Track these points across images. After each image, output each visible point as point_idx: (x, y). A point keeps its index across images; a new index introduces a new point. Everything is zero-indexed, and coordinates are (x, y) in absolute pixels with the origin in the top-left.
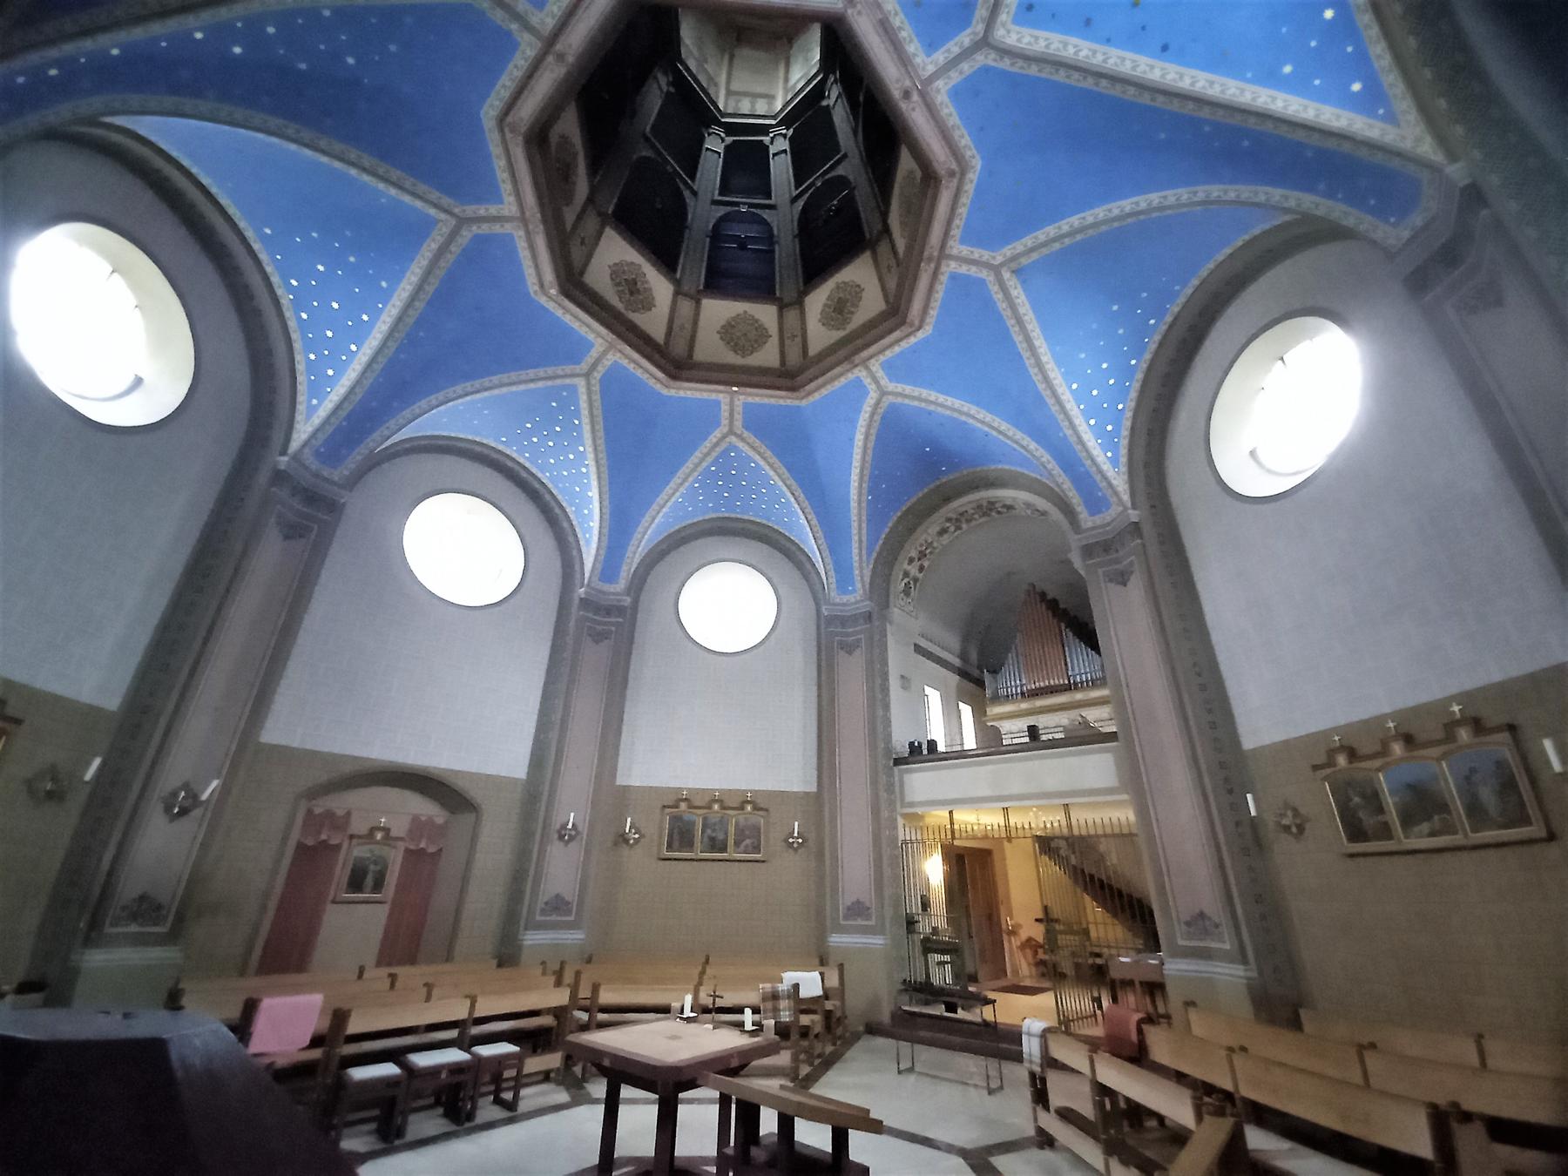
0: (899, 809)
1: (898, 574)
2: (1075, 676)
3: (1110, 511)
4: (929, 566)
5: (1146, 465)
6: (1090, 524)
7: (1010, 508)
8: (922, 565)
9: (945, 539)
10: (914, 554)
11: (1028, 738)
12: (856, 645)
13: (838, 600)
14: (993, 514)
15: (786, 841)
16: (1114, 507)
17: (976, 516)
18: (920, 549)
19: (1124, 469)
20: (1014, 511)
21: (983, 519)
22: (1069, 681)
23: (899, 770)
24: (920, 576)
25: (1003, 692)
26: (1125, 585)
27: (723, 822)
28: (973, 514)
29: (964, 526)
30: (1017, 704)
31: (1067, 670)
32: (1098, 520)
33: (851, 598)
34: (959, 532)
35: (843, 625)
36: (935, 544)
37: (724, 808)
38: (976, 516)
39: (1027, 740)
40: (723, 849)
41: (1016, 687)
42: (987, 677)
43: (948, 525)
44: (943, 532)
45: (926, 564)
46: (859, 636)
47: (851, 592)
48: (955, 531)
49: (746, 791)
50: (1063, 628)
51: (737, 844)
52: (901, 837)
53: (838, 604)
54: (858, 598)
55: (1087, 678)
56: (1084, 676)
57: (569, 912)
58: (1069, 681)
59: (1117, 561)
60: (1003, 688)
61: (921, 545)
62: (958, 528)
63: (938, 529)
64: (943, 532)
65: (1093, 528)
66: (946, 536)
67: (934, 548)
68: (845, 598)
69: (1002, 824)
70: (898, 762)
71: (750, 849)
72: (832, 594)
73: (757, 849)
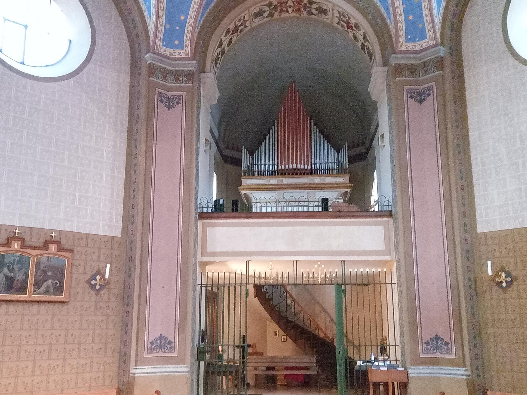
4: (235, 42)
5: (454, 14)
6: (404, 48)
8: (231, 39)
10: (232, 27)
12: (178, 100)
13: (162, 51)
14: (305, 13)
15: (89, 282)
16: (428, 39)
18: (237, 23)
19: (441, 11)
20: (324, 16)
21: (294, 14)
22: (312, 167)
24: (226, 49)
25: (256, 168)
27: (23, 262)
28: (290, 7)
29: (276, 15)
31: (311, 158)
32: (411, 46)
33: (177, 53)
34: (269, 18)
36: (248, 24)
37: (23, 246)
38: (290, 10)
39: (320, 209)
40: (23, 289)
41: (269, 165)
43: (267, 9)
44: (259, 14)
45: (234, 40)
47: (176, 47)
49: (52, 231)
51: (38, 284)
54: (183, 55)
55: (325, 166)
58: (312, 167)
59: (417, 83)
61: (239, 21)
63: (257, 10)
66: (258, 19)
67: (246, 27)
68: (169, 51)
69: (244, 273)
70: (202, 216)
71: (52, 290)
72: (158, 43)
73: (59, 290)
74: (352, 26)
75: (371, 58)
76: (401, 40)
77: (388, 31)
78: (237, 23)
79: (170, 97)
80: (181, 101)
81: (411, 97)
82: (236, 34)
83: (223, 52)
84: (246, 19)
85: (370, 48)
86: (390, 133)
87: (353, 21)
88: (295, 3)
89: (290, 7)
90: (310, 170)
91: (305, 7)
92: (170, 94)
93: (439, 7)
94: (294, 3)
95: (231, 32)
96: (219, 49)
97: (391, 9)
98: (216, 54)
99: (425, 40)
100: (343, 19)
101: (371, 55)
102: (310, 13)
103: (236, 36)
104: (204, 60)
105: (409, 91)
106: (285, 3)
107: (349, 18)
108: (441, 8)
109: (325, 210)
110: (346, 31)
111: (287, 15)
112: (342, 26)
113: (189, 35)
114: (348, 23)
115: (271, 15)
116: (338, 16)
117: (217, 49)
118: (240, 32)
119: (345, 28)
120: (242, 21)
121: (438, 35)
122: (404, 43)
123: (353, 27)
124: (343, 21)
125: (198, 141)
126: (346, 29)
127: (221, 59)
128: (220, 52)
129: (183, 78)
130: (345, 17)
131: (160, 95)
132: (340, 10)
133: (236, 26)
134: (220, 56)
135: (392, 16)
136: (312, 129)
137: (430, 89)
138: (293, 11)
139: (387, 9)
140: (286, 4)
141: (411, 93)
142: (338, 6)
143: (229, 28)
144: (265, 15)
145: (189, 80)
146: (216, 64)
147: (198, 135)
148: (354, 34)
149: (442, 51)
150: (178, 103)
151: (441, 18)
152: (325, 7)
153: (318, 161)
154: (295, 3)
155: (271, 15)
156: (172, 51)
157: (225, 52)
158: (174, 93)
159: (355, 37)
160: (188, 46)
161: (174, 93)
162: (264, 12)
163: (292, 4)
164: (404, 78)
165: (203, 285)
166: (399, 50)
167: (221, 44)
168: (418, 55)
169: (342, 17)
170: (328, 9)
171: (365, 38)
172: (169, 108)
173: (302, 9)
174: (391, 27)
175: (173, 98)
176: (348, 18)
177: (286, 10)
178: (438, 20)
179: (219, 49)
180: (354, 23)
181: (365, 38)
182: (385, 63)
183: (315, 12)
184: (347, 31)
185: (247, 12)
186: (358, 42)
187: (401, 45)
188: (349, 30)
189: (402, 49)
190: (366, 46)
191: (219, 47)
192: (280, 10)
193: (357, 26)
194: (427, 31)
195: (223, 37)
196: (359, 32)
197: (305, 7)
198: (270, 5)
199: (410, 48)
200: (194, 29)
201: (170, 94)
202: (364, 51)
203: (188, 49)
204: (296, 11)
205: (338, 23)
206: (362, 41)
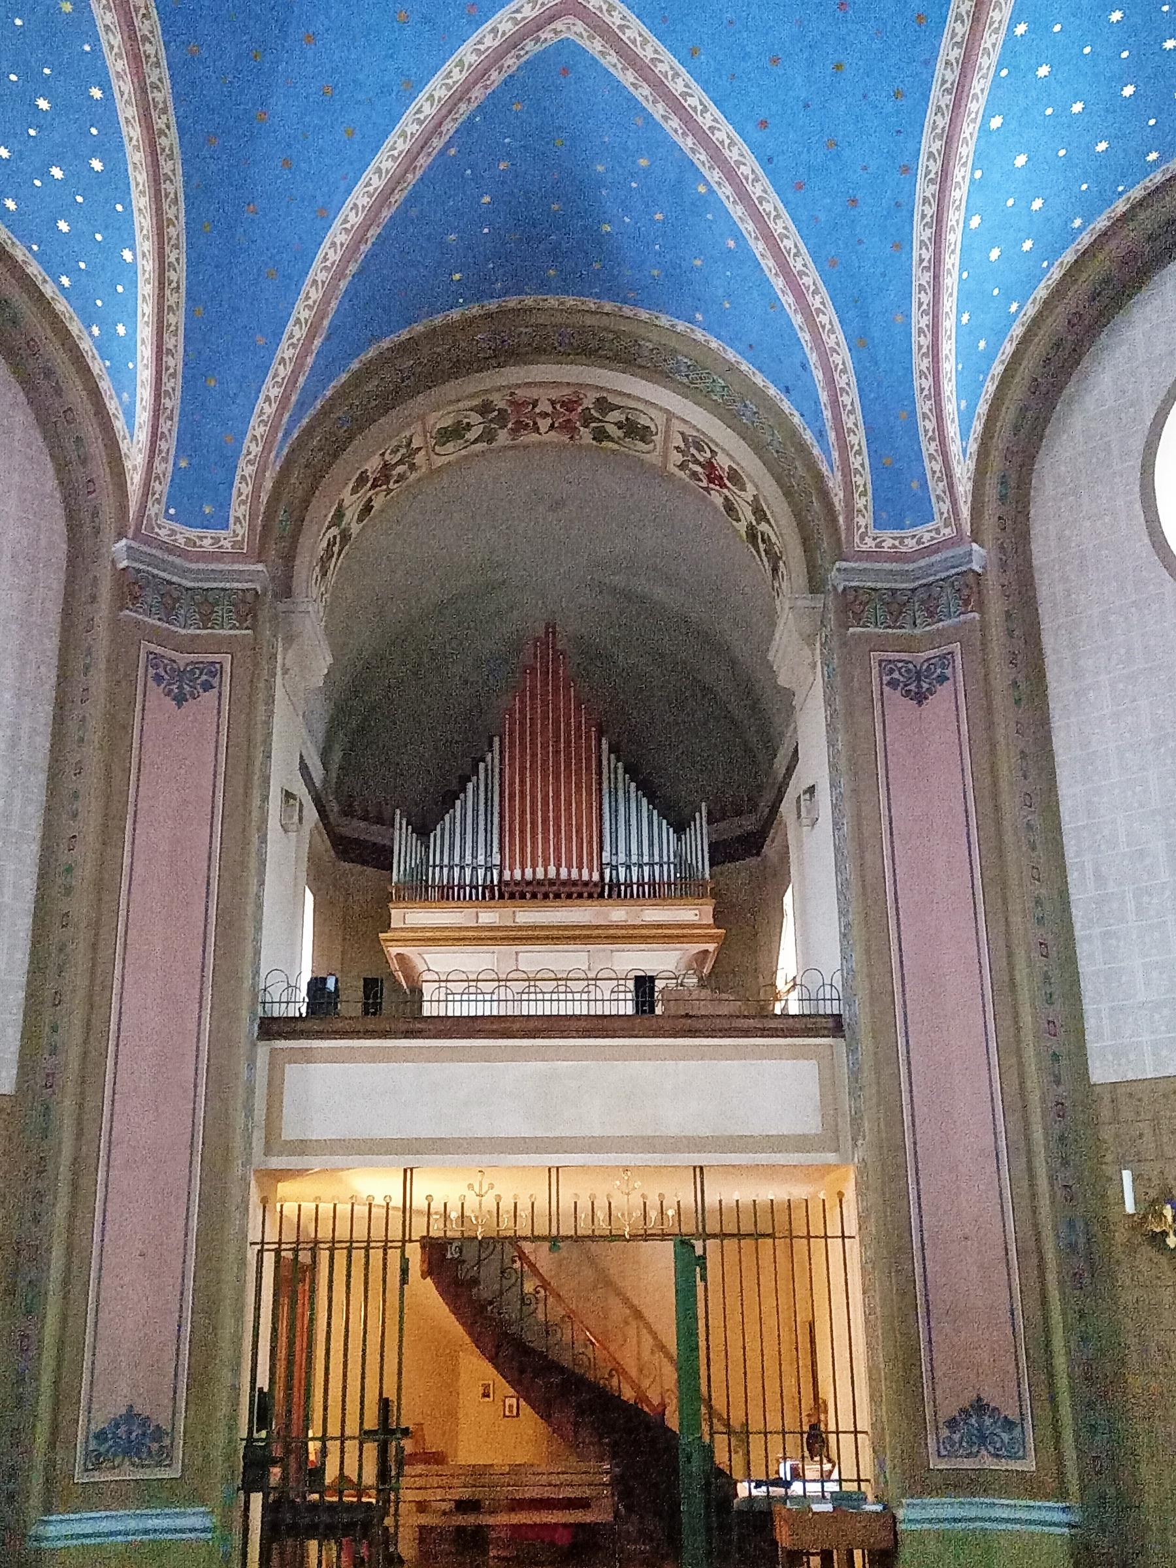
1: (321, 510)
3: (919, 530)
5: (1009, 454)
6: (869, 544)
7: (634, 430)
8: (370, 500)
9: (451, 451)
10: (373, 465)
16: (938, 522)
17: (544, 424)
19: (973, 447)
20: (641, 446)
24: (355, 528)
25: (437, 876)
26: (920, 703)
28: (545, 415)
29: (503, 437)
31: (601, 849)
35: (169, 611)
36: (419, 459)
38: (544, 424)
39: (629, 1009)
41: (474, 869)
42: (403, 842)
43: (475, 418)
44: (455, 432)
45: (377, 504)
46: (143, 655)
48: (475, 441)
50: (605, 746)
53: (171, 549)
57: (163, 1457)
60: (434, 866)
61: (395, 451)
63: (448, 422)
64: (455, 432)
65: (869, 556)
66: (450, 447)
67: (413, 467)
68: (183, 534)
69: (397, 1202)
74: (721, 478)
75: (775, 570)
77: (824, 495)
78: (387, 457)
80: (215, 682)
81: (893, 684)
82: (384, 487)
83: (345, 536)
84: (414, 446)
85: (774, 539)
87: (722, 461)
88: (558, 406)
89: (545, 415)
90: (596, 885)
92: (183, 659)
93: (964, 435)
95: (369, 485)
96: (334, 531)
97: (832, 436)
98: (324, 544)
99: (930, 526)
101: (775, 559)
102: (601, 435)
104: (289, 558)
108: (971, 439)
109: (644, 1012)
111: (535, 437)
112: (694, 475)
113: (247, 490)
114: (710, 466)
115: (488, 436)
116: (682, 446)
117: (329, 528)
119: (700, 480)
120: (403, 451)
121: (965, 512)
124: (697, 462)
125: (265, 798)
126: (704, 484)
127: (339, 555)
128: (335, 537)
130: (700, 450)
131: (155, 660)
133: (385, 465)
134: (336, 549)
135: (835, 454)
136: (605, 762)
137: (946, 659)
138: (552, 426)
139: (821, 435)
140: (534, 407)
141: (891, 671)
144: (471, 435)
145: (242, 619)
147: (266, 780)
148: (726, 498)
149: (979, 556)
150: (207, 686)
151: (972, 466)
152: (643, 421)
153: (622, 858)
154: (558, 406)
155: (488, 436)
156: (193, 533)
159: (730, 508)
163: (549, 410)
164: (872, 629)
165: (266, 1247)
167: (339, 514)
168: (910, 567)
169: (693, 451)
170: (653, 429)
172: (180, 700)
174: (835, 483)
175: (192, 672)
176: (708, 455)
178: (963, 470)
179: (334, 531)
182: (815, 585)
184: (706, 489)
185: (417, 427)
188: (711, 486)
189: (864, 548)
193: (734, 477)
194: (933, 500)
195: (346, 494)
196: (742, 494)
197: (587, 420)
201: (183, 659)
203: (242, 530)
204: (561, 427)
205: (682, 466)
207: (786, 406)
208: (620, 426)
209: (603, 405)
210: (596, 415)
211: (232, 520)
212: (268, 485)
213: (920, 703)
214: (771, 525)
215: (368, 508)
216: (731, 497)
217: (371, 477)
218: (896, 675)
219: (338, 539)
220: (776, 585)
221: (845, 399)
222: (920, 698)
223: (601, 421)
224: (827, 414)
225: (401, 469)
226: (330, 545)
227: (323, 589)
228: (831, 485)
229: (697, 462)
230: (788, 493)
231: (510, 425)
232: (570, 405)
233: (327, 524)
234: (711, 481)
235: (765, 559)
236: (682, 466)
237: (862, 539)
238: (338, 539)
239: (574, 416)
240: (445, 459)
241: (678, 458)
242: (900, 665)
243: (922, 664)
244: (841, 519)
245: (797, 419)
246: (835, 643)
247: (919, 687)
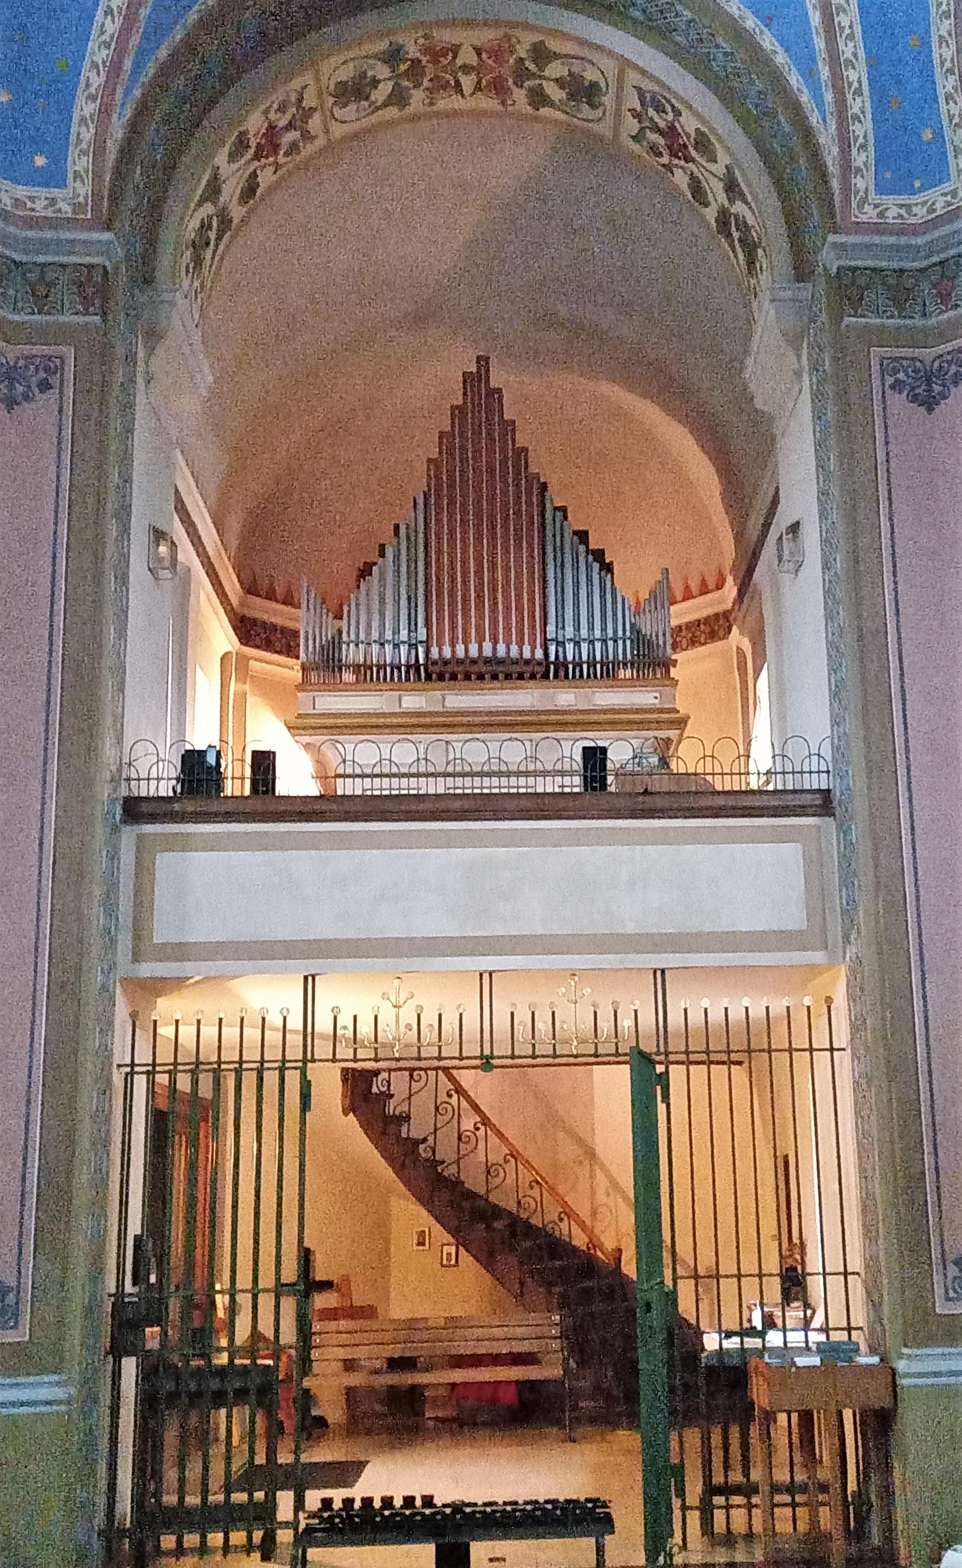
0: (124, 966)
2: (560, 644)
3: (931, 195)
4: (271, 189)
6: (869, 214)
8: (254, 175)
10: (255, 124)
11: (577, 780)
14: (520, 96)
18: (272, 116)
20: (586, 110)
23: (140, 837)
26: (930, 410)
28: (466, 69)
29: (418, 97)
30: (396, 694)
36: (315, 123)
38: (468, 82)
43: (382, 71)
52: (121, 1055)
56: (584, 646)
61: (282, 109)
62: (398, 98)
63: (346, 74)
74: (685, 146)
75: (751, 262)
76: (859, 183)
77: (815, 154)
78: (272, 116)
79: (12, 363)
81: (897, 386)
82: (271, 159)
83: (225, 222)
85: (750, 220)
86: (823, 515)
87: (689, 124)
88: (484, 56)
89: (466, 69)
91: (521, 74)
94: (479, 54)
95: (252, 151)
97: (825, 73)
98: (195, 224)
100: (657, 119)
101: (750, 248)
102: (538, 98)
103: (272, 169)
105: (890, 366)
106: (450, 57)
107: (677, 113)
110: (664, 165)
111: (456, 102)
112: (654, 150)
113: (88, 135)
114: (671, 132)
116: (639, 108)
117: (200, 204)
118: (287, 154)
119: (660, 154)
122: (872, 194)
123: (691, 149)
124: (657, 129)
125: (125, 531)
126: (665, 160)
127: (217, 246)
128: (210, 217)
129: (65, 293)
130: (660, 110)
132: (648, 86)
133: (271, 127)
134: (212, 235)
135: (829, 97)
138: (478, 88)
139: (810, 74)
141: (895, 371)
142: (637, 67)
143: (242, 134)
146: (198, 261)
147: (124, 512)
150: (45, 386)
152: (590, 75)
155: (398, 98)
157: (233, 225)
158: (27, 349)
160: (85, 177)
161: (27, 349)
162: (375, 83)
163: (473, 60)
166: (853, 219)
167: (213, 190)
168: (920, 241)
169: (651, 112)
170: (603, 85)
171: (732, 187)
173: (510, 81)
174: (827, 137)
176: (670, 116)
177: (452, 83)
179: (208, 208)
180: (693, 134)
181: (732, 187)
183: (555, 93)
184: (668, 168)
186: (706, 205)
187: (864, 201)
188: (676, 161)
189: (864, 218)
190: (736, 217)
191: (206, 200)
192: (431, 80)
193: (703, 143)
195: (221, 159)
196: (712, 167)
197: (521, 74)
198: (393, 56)
199: (890, 214)
200: (105, 111)
202: (729, 235)
205: (637, 138)
206: (722, 197)
207: (768, 41)
208: (560, 82)
209: (541, 54)
210: (532, 67)
211: (70, 175)
212: (117, 132)
213: (930, 410)
214: (747, 203)
215: (250, 190)
216: (695, 170)
217: (253, 144)
218: (901, 376)
219: (215, 224)
220: (753, 281)
221: (843, 20)
222: (929, 403)
223: (540, 77)
224: (819, 43)
225: (293, 135)
226: (205, 226)
227: (196, 284)
228: (822, 141)
229: (657, 129)
230: (766, 155)
231: (426, 83)
232: (497, 53)
233: (197, 198)
234: (674, 154)
235: (739, 250)
236: (637, 138)
237: (861, 205)
238: (215, 224)
239: (505, 71)
240: (347, 128)
241: (633, 125)
242: (904, 363)
243: (933, 362)
244: (835, 184)
245: (781, 58)
246: (825, 339)
247: (930, 390)
